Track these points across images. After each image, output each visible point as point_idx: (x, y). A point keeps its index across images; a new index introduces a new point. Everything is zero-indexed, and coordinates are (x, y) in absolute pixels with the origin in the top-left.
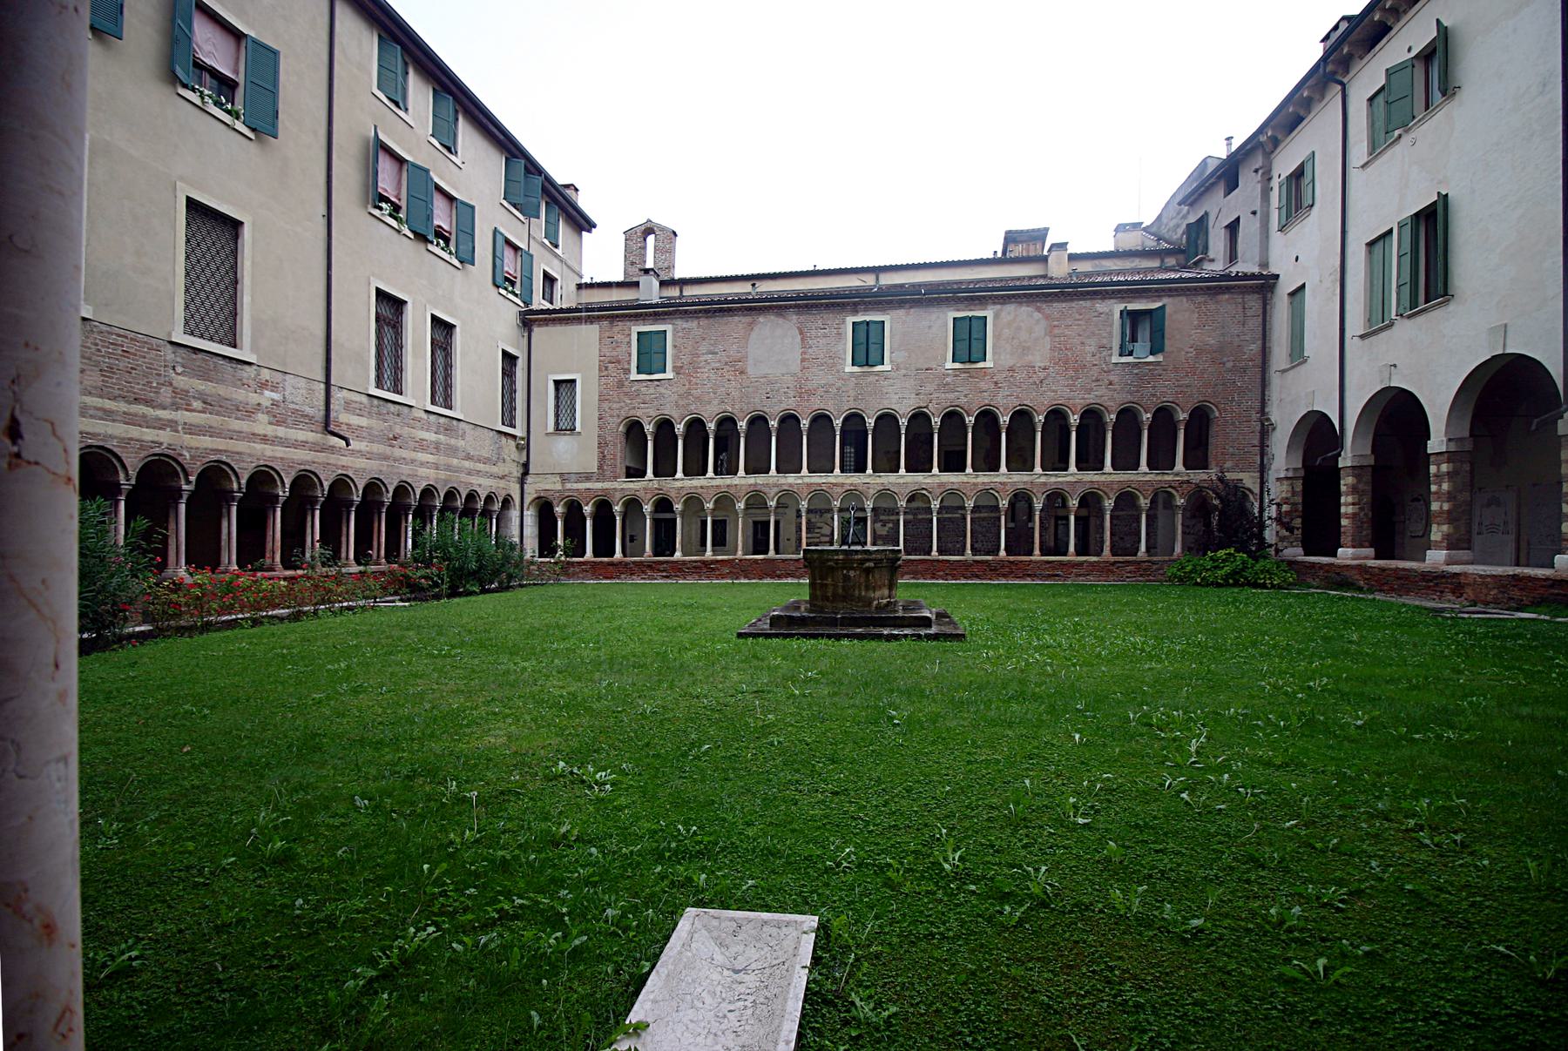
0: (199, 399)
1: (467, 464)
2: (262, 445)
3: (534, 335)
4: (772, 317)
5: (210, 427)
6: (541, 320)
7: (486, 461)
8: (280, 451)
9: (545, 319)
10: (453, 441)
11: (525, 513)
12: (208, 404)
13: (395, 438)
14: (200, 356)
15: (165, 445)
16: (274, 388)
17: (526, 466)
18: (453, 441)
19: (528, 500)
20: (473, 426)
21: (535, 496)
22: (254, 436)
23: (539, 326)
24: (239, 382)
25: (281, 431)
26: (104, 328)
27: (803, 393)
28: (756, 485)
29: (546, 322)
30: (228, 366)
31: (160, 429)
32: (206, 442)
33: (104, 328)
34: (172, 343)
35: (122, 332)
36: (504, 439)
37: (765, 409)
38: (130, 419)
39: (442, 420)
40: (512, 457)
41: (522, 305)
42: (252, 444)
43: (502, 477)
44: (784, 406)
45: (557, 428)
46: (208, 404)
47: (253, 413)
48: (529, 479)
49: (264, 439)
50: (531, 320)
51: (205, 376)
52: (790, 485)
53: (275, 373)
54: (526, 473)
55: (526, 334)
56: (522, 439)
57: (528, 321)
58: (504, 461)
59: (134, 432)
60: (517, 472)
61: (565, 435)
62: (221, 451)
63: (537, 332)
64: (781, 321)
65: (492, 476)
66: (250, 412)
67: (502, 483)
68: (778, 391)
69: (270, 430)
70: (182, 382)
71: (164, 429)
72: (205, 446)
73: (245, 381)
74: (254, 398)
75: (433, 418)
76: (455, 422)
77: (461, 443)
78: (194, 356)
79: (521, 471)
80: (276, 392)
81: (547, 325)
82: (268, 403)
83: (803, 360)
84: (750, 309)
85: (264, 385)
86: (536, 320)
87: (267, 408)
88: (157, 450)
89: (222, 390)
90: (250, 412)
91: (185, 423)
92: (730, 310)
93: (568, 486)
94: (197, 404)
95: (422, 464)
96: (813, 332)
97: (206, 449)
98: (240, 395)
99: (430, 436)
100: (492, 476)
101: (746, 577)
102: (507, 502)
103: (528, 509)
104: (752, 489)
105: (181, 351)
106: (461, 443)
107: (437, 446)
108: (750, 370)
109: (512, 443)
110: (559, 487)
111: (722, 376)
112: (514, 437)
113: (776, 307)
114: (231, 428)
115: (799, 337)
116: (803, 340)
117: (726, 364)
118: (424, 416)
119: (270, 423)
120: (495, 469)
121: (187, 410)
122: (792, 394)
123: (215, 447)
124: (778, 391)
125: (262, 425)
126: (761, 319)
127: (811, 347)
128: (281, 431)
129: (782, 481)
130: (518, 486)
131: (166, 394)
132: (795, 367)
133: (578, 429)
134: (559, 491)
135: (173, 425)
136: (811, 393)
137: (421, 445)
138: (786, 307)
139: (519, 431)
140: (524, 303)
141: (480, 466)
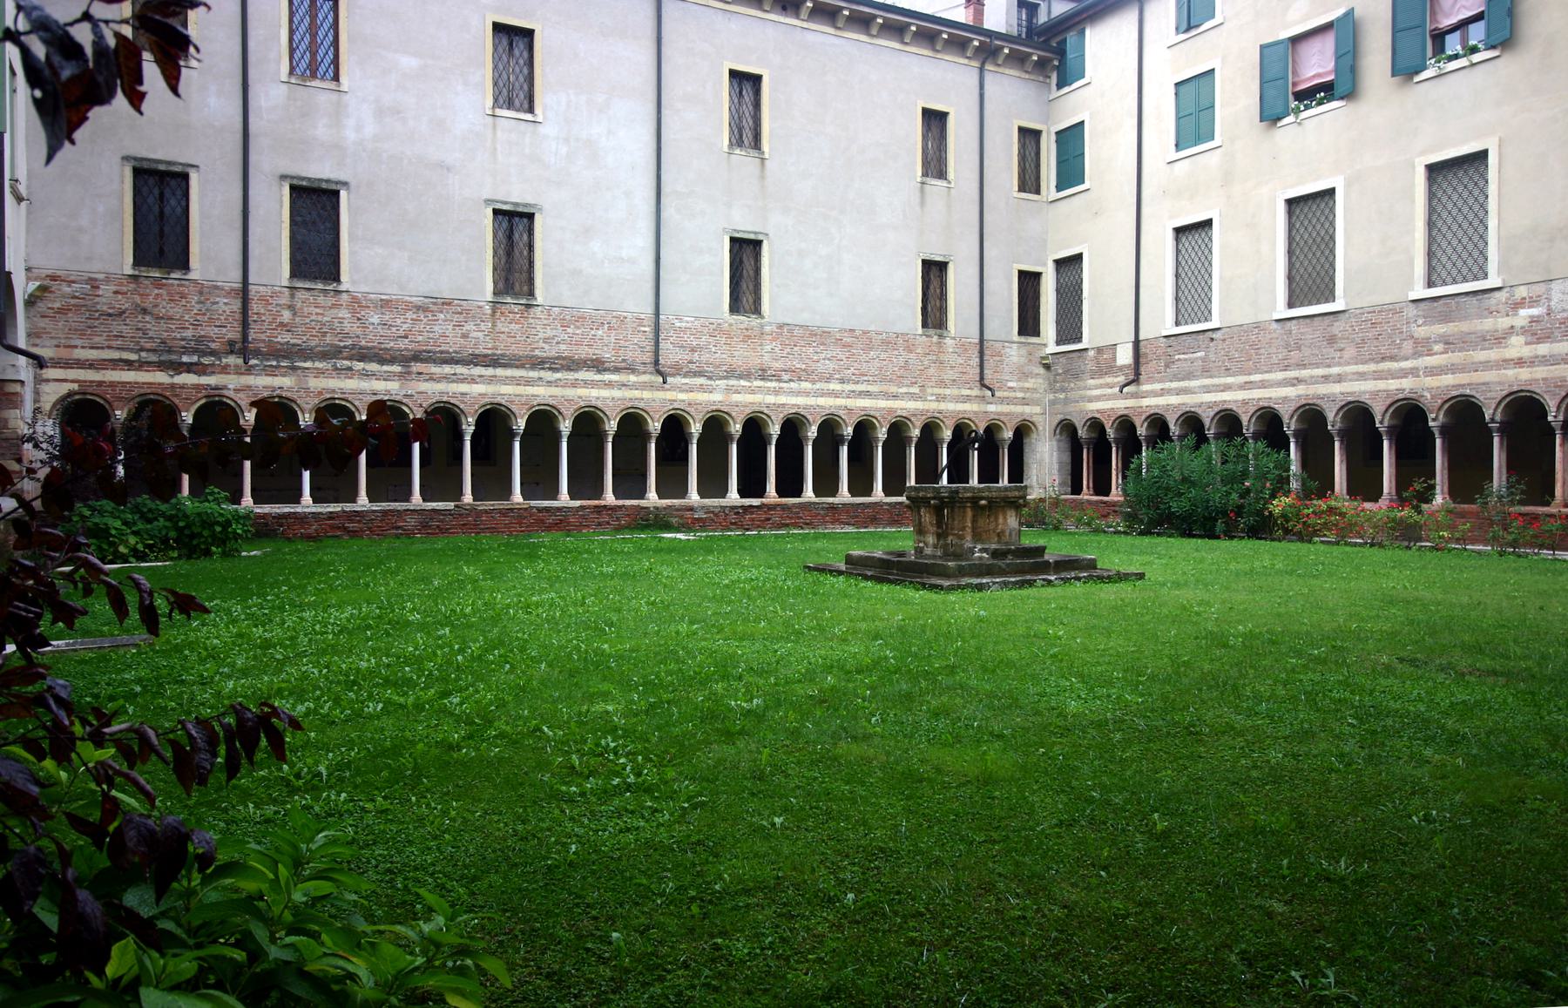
0: (1439, 342)
2: (1516, 370)
5: (1453, 365)
8: (1540, 372)
12: (1449, 343)
14: (1441, 302)
15: (1408, 390)
16: (1533, 302)
22: (1506, 363)
24: (1486, 312)
25: (1543, 349)
26: (1358, 311)
30: (1474, 300)
31: (1402, 378)
32: (1448, 380)
33: (1358, 311)
35: (1371, 309)
38: (1379, 376)
42: (1503, 371)
46: (1449, 343)
47: (1504, 338)
49: (1520, 362)
51: (1446, 318)
53: (1534, 287)
59: (1381, 385)
62: (1464, 385)
66: (1500, 339)
69: (1527, 352)
70: (1421, 332)
71: (1406, 377)
72: (1446, 383)
73: (1494, 308)
74: (1504, 323)
78: (1436, 304)
80: (1538, 306)
82: (1524, 323)
85: (1521, 304)
87: (1522, 328)
88: (1401, 396)
89: (1464, 326)
90: (1500, 339)
91: (1426, 368)
94: (1437, 348)
97: (1447, 386)
98: (1487, 324)
105: (1422, 305)
114: (1476, 360)
119: (1527, 344)
123: (1457, 382)
125: (1517, 347)
128: (1543, 349)
131: (1408, 347)
135: (1414, 372)
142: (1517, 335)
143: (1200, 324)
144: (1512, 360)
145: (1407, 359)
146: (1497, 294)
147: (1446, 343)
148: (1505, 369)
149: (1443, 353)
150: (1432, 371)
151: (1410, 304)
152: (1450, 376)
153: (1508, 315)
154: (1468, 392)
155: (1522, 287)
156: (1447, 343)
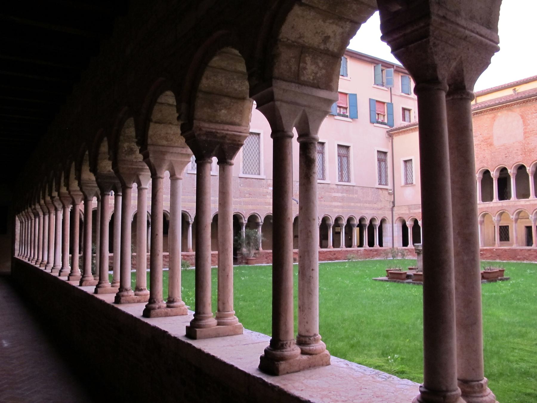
1: (359, 205)
2: (269, 206)
3: (394, 140)
4: (505, 112)
6: (396, 133)
7: (370, 202)
9: (398, 133)
10: (351, 196)
11: (394, 225)
13: (322, 198)
14: (248, 180)
15: (238, 209)
17: (394, 203)
18: (351, 196)
19: (395, 218)
20: (362, 188)
21: (398, 217)
23: (396, 136)
27: (526, 151)
28: (502, 206)
29: (398, 133)
32: (250, 207)
34: (239, 177)
36: (380, 191)
37: (505, 163)
39: (345, 187)
40: (386, 199)
41: (389, 127)
42: (265, 206)
43: (381, 209)
44: (515, 160)
45: (406, 183)
47: (265, 195)
48: (395, 209)
50: (392, 134)
52: (522, 206)
54: (394, 206)
55: (391, 141)
56: (391, 190)
57: (390, 135)
58: (381, 201)
60: (390, 205)
61: (409, 186)
63: (396, 139)
64: (510, 113)
65: (373, 209)
67: (380, 212)
68: (512, 152)
75: (339, 187)
76: (351, 187)
77: (355, 196)
78: (246, 180)
79: (392, 205)
81: (399, 135)
83: (525, 133)
84: (492, 110)
86: (394, 133)
92: (481, 112)
93: (412, 211)
94: (247, 195)
95: (336, 207)
96: (530, 116)
99: (340, 195)
100: (373, 209)
101: (500, 259)
102: (383, 221)
103: (395, 223)
104: (500, 209)
105: (242, 179)
106: (355, 196)
107: (342, 199)
108: (496, 143)
109: (386, 193)
110: (407, 212)
111: (481, 148)
112: (387, 189)
113: (506, 106)
115: (521, 121)
116: (524, 121)
117: (482, 141)
118: (336, 187)
120: (375, 206)
121: (244, 198)
122: (520, 153)
124: (512, 152)
126: (499, 114)
127: (528, 125)
129: (518, 203)
130: (391, 212)
132: (520, 137)
133: (414, 183)
134: (408, 214)
136: (531, 151)
137: (335, 199)
138: (512, 105)
139: (390, 187)
140: (390, 126)
141: (367, 205)
142: (269, 195)
143: (249, 175)
144: (267, 203)
145: (237, 198)
146: (263, 180)
147: (250, 194)
148: (266, 206)
149: (248, 198)
150: (247, 203)
151: (238, 178)
152: (251, 206)
153: (266, 188)
154: (256, 212)
155: (269, 180)
156: (250, 194)
